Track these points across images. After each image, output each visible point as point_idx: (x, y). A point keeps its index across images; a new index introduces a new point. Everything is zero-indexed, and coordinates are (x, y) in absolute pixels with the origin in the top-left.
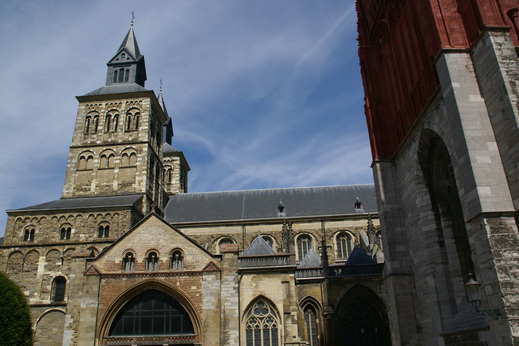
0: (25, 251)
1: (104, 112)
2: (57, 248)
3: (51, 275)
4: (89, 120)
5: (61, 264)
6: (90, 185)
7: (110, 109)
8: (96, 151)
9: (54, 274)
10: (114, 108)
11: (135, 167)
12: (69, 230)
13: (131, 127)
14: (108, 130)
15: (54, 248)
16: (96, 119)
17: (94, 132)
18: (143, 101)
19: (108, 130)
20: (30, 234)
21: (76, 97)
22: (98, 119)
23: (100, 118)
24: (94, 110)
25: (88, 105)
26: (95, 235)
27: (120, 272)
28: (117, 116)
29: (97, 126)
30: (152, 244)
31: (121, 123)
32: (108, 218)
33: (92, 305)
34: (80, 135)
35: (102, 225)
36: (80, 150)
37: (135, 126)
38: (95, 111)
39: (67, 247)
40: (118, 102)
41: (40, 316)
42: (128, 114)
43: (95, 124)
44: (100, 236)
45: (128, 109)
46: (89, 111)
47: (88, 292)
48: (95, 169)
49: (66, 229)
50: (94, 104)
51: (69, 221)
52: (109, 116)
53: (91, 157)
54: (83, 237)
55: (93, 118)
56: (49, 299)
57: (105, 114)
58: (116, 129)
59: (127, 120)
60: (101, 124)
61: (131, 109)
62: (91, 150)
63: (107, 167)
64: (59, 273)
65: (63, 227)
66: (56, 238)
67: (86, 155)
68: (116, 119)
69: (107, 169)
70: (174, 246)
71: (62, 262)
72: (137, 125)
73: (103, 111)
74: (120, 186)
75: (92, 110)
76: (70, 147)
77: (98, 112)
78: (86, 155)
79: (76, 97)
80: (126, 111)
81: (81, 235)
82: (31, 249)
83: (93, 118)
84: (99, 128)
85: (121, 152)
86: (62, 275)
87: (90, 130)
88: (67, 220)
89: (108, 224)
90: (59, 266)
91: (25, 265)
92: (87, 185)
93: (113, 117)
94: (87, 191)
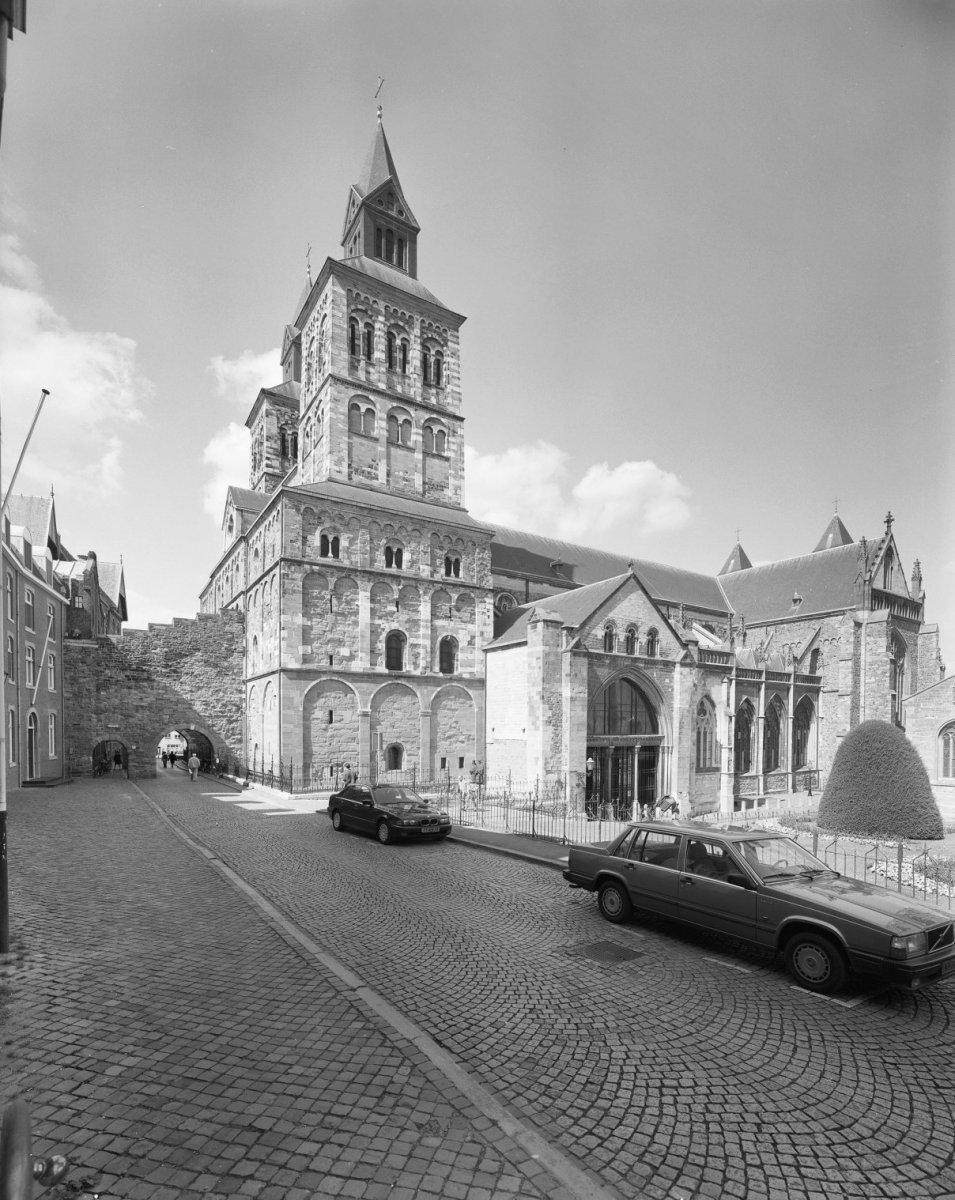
3: (382, 626)
5: (395, 609)
6: (376, 469)
7: (392, 321)
9: (388, 626)
10: (401, 324)
12: (400, 552)
18: (449, 333)
26: (443, 571)
27: (602, 652)
30: (634, 620)
33: (582, 695)
36: (352, 392)
39: (403, 582)
40: (408, 314)
41: (375, 692)
44: (448, 573)
45: (425, 336)
47: (576, 675)
49: (395, 550)
51: (399, 536)
54: (425, 571)
56: (384, 665)
61: (428, 338)
64: (395, 626)
66: (380, 564)
70: (651, 624)
71: (397, 607)
81: (421, 567)
86: (401, 629)
88: (396, 534)
90: (394, 612)
91: (334, 601)
92: (371, 467)
94: (372, 478)
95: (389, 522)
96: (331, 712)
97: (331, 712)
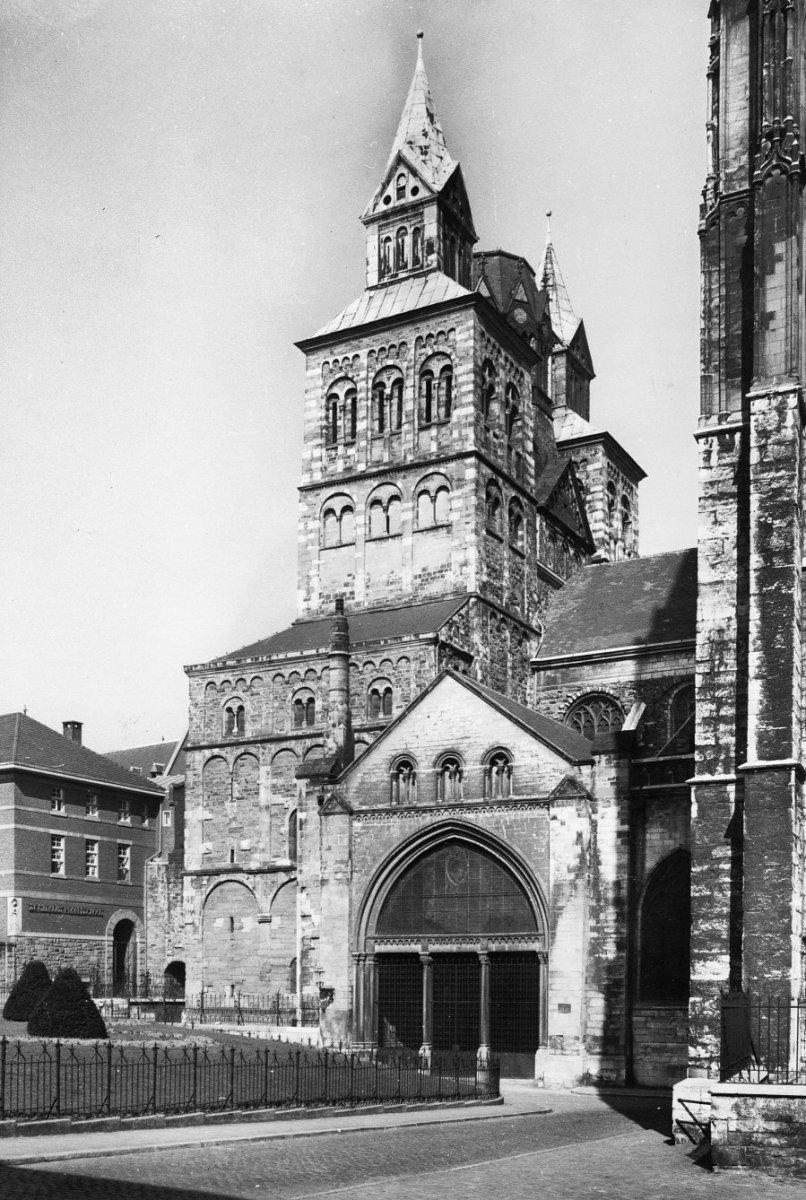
0: (230, 754)
1: (366, 379)
2: (291, 744)
4: (335, 404)
7: (378, 367)
8: (359, 493)
10: (390, 362)
11: (448, 526)
12: (311, 700)
13: (434, 412)
14: (382, 428)
15: (284, 745)
16: (349, 401)
17: (349, 439)
19: (382, 428)
20: (237, 716)
21: (296, 344)
22: (354, 401)
23: (359, 396)
24: (342, 374)
25: (327, 363)
28: (399, 383)
29: (354, 420)
31: (408, 406)
32: (387, 670)
34: (316, 450)
35: (376, 686)
37: (443, 410)
38: (345, 378)
42: (425, 373)
43: (349, 416)
46: (332, 381)
48: (360, 542)
50: (340, 358)
52: (378, 386)
53: (347, 509)
55: (342, 397)
57: (370, 382)
58: (400, 425)
59: (424, 393)
60: (361, 413)
62: (346, 491)
63: (386, 534)
65: (297, 697)
67: (337, 504)
68: (396, 394)
69: (387, 538)
72: (449, 405)
73: (363, 374)
74: (419, 581)
75: (338, 376)
76: (301, 489)
77: (351, 380)
78: (337, 504)
79: (296, 344)
80: (418, 366)
82: (242, 750)
83: (342, 397)
84: (361, 426)
85: (413, 489)
87: (340, 435)
89: (388, 685)
92: (346, 585)
93: (388, 391)
95: (294, 670)
96: (232, 918)
97: (232, 918)
